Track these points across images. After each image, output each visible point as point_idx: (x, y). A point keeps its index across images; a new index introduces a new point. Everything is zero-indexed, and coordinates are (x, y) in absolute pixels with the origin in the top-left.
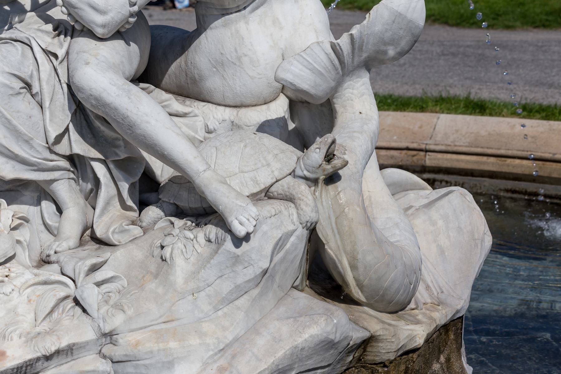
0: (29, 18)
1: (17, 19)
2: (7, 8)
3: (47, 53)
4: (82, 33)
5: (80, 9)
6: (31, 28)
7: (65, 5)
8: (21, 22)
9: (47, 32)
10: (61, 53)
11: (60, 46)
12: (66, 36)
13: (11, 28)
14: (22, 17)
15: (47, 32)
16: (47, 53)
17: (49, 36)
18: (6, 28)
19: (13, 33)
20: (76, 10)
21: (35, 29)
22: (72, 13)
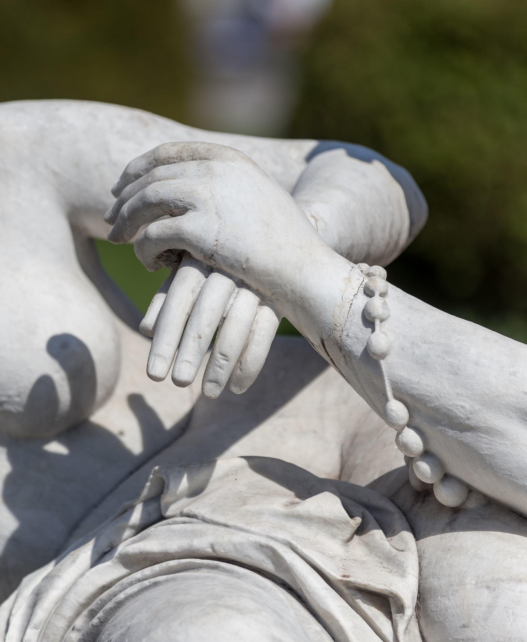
0: (221, 478)
1: (184, 483)
2: (55, 447)
3: (356, 593)
4: (462, 519)
5: (489, 431)
6: (260, 513)
7: (418, 421)
8: (195, 492)
9: (326, 523)
10: (406, 589)
11: (395, 563)
12: (389, 532)
13: (156, 517)
14: (200, 477)
15: (326, 523)
16: (356, 593)
17: (334, 536)
18: (136, 516)
19: (195, 534)
20: (468, 437)
21: (276, 514)
22: (436, 448)
